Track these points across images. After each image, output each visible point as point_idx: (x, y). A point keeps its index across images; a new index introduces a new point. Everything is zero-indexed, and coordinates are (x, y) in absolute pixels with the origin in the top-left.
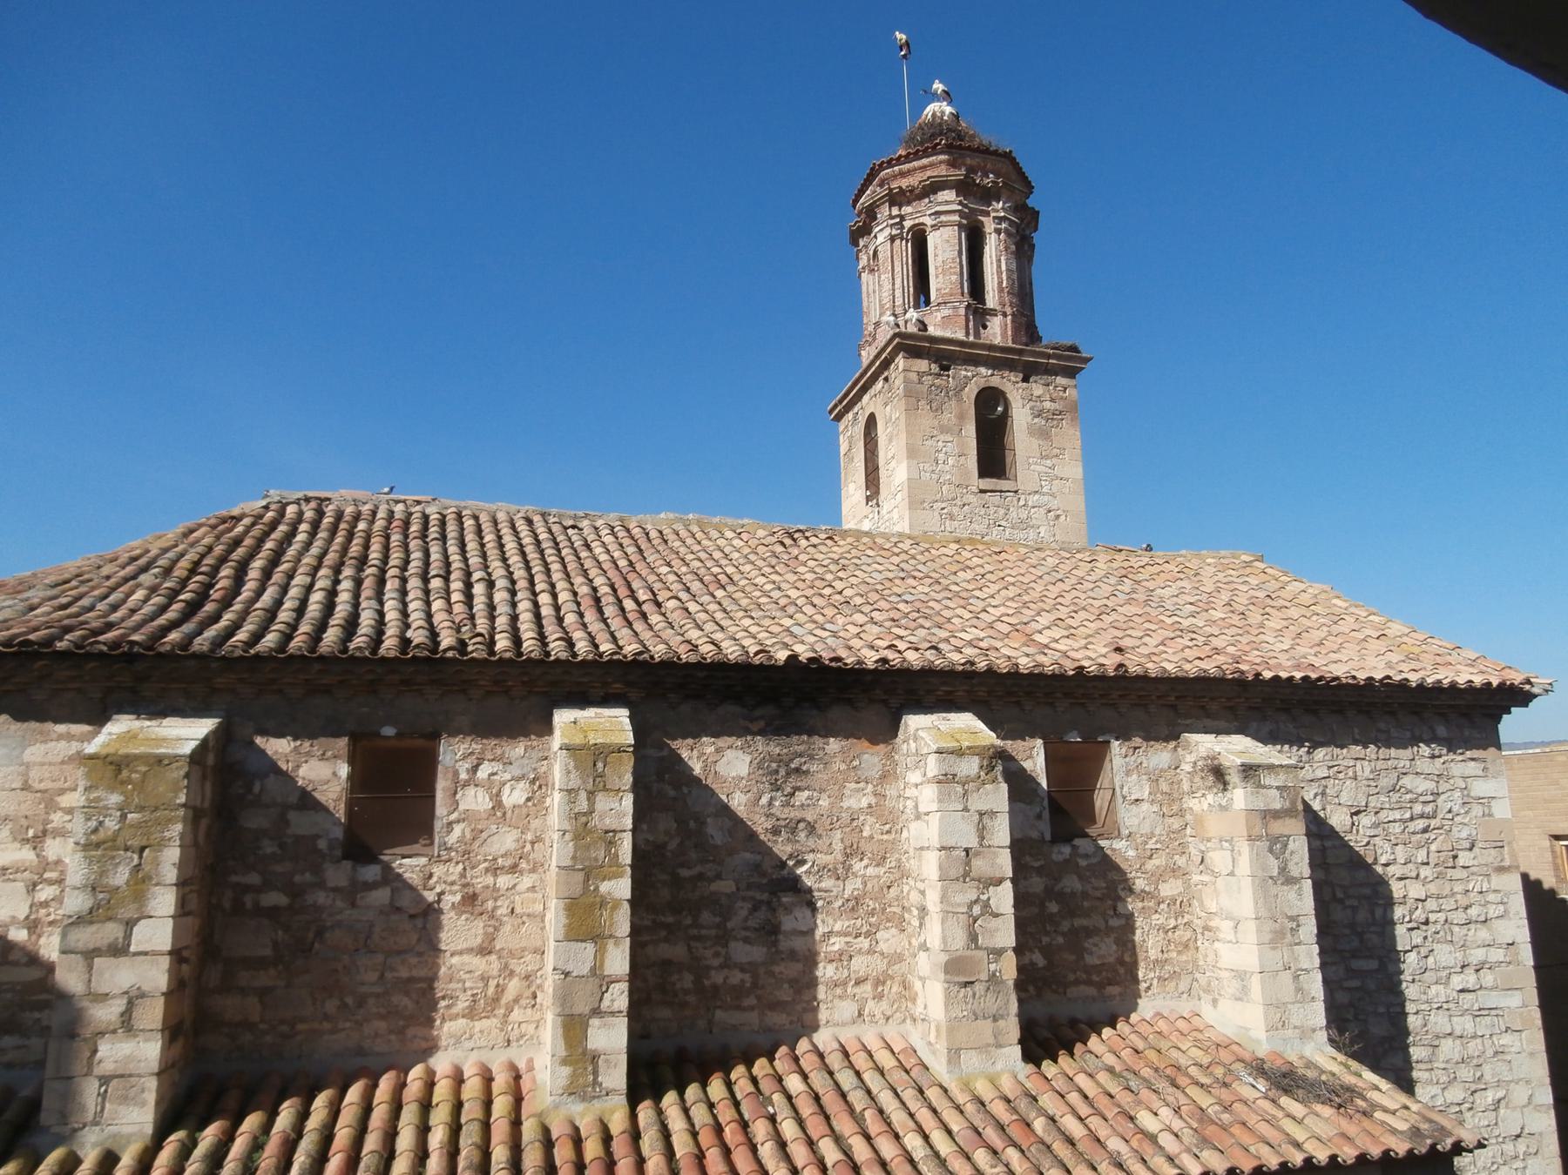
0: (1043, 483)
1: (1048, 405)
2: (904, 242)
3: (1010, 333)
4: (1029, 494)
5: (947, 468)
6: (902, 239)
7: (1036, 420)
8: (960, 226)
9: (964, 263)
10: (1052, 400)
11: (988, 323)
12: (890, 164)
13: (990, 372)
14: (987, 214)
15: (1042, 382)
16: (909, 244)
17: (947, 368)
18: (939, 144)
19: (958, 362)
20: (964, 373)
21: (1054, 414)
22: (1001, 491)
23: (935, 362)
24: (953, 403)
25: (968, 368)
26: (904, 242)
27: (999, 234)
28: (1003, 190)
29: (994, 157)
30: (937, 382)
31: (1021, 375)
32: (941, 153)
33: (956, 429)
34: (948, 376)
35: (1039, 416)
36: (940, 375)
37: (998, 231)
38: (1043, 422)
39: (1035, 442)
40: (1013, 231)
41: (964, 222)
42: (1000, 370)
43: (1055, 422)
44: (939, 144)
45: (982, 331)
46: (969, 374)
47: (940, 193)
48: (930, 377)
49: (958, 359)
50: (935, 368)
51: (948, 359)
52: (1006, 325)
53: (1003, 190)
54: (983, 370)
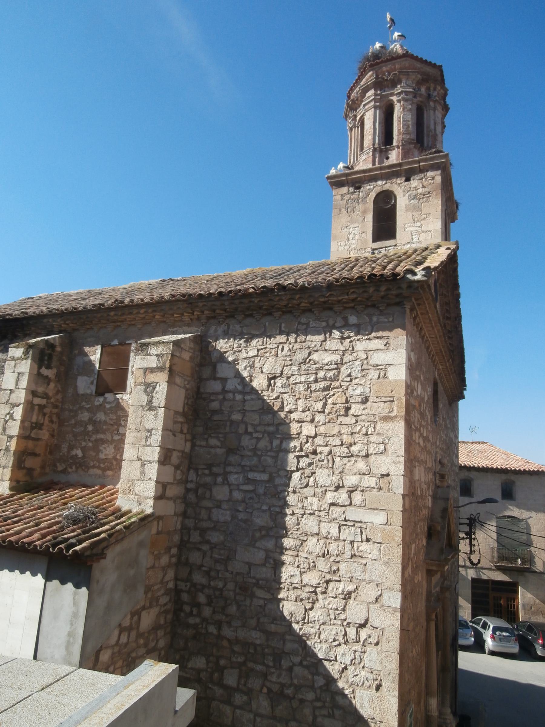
0: (414, 237)
1: (420, 191)
2: (356, 128)
3: (401, 157)
4: (404, 245)
5: (354, 241)
6: (355, 127)
7: (412, 201)
8: (375, 107)
9: (377, 127)
10: (424, 187)
11: (390, 156)
12: (352, 89)
13: (384, 182)
14: (392, 94)
15: (418, 178)
16: (359, 129)
17: (359, 188)
18: (366, 67)
19: (365, 182)
20: (368, 187)
21: (424, 195)
22: (386, 247)
23: (352, 186)
24: (361, 206)
25: (371, 184)
26: (356, 128)
27: (400, 102)
28: (401, 76)
29: (398, 60)
30: (352, 197)
31: (404, 179)
32: (370, 71)
33: (361, 219)
34: (359, 192)
35: (414, 198)
36: (355, 192)
37: (399, 101)
38: (417, 201)
39: (410, 215)
40: (410, 97)
41: (378, 104)
42: (390, 179)
43: (425, 199)
44: (366, 67)
45: (385, 160)
46: (372, 187)
47: (367, 94)
48: (348, 195)
49: (365, 180)
50: (351, 189)
51: (357, 182)
52: (399, 153)
53: (401, 76)
54: (380, 183)
